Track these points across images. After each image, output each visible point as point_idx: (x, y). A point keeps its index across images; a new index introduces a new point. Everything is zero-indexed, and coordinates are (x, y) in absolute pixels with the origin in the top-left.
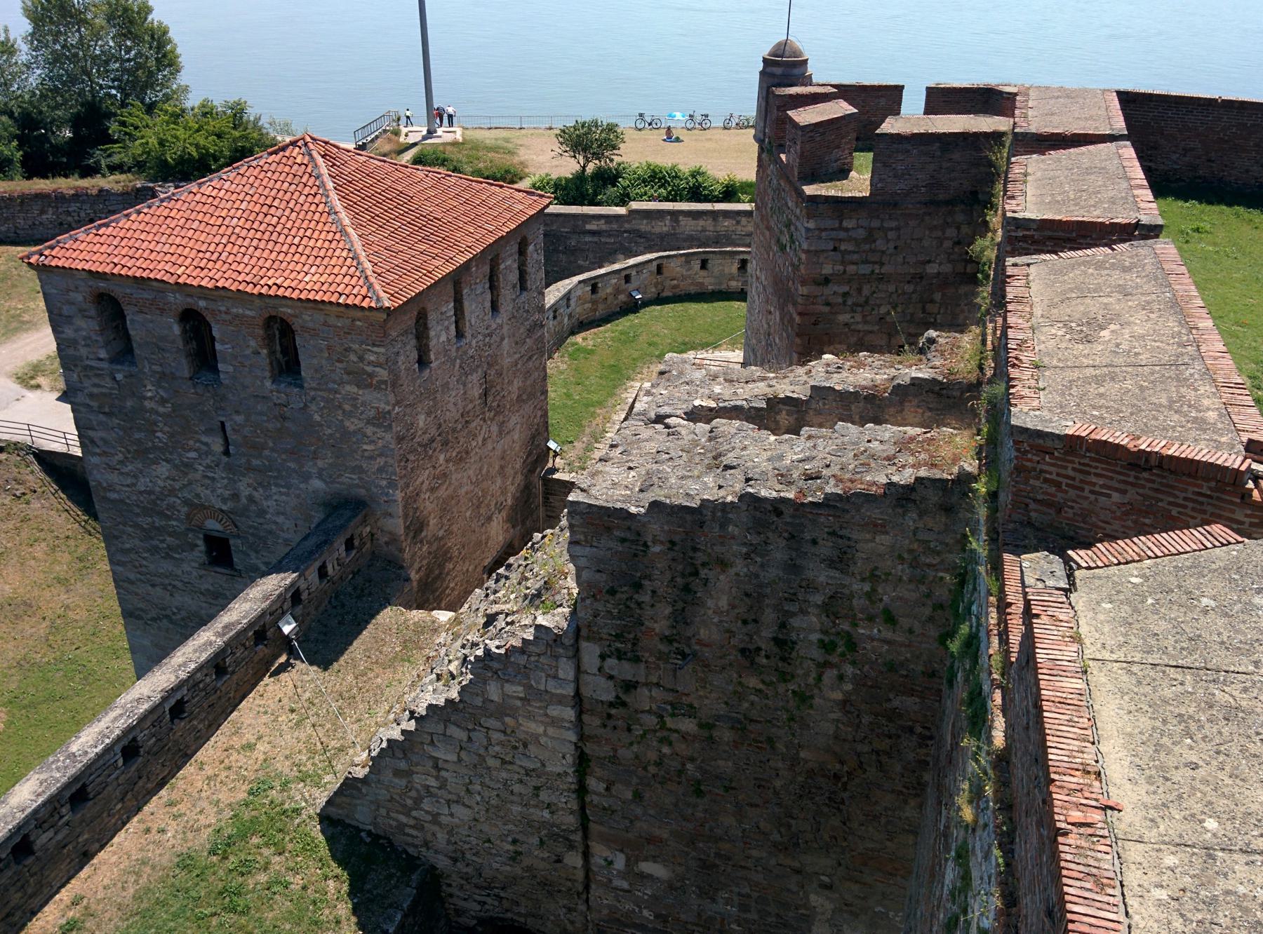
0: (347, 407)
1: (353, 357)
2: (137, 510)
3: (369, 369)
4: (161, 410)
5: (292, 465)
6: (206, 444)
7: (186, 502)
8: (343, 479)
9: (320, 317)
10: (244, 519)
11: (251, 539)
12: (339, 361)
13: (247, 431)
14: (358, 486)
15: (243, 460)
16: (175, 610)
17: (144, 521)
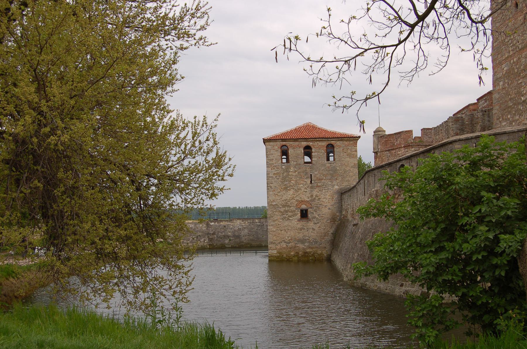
0: (346, 164)
1: (349, 151)
2: (281, 206)
3: (353, 153)
4: (294, 174)
5: (329, 183)
6: (306, 182)
7: (297, 201)
8: (343, 184)
9: (341, 142)
10: (313, 202)
11: (315, 208)
12: (345, 153)
13: (318, 176)
14: (348, 185)
15: (316, 184)
16: (287, 238)
17: (282, 210)
